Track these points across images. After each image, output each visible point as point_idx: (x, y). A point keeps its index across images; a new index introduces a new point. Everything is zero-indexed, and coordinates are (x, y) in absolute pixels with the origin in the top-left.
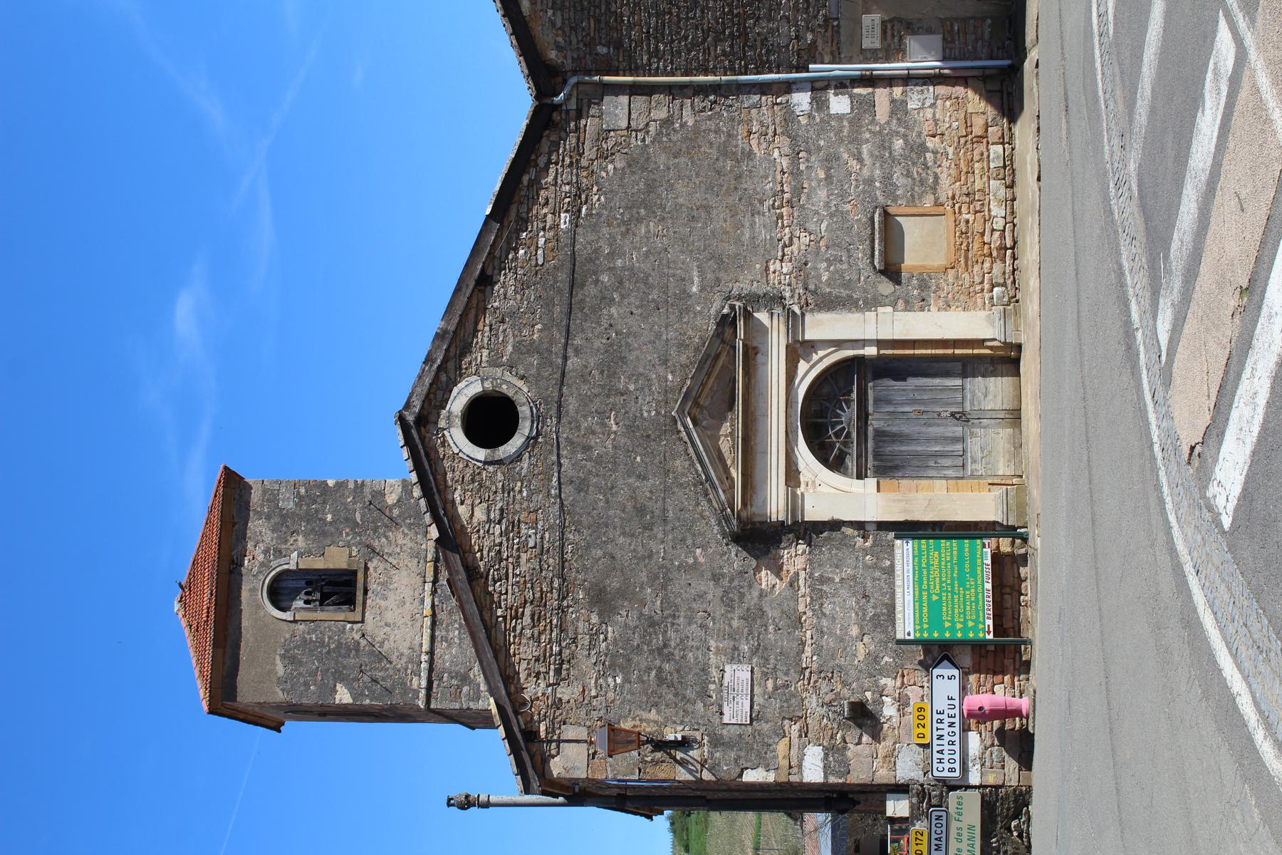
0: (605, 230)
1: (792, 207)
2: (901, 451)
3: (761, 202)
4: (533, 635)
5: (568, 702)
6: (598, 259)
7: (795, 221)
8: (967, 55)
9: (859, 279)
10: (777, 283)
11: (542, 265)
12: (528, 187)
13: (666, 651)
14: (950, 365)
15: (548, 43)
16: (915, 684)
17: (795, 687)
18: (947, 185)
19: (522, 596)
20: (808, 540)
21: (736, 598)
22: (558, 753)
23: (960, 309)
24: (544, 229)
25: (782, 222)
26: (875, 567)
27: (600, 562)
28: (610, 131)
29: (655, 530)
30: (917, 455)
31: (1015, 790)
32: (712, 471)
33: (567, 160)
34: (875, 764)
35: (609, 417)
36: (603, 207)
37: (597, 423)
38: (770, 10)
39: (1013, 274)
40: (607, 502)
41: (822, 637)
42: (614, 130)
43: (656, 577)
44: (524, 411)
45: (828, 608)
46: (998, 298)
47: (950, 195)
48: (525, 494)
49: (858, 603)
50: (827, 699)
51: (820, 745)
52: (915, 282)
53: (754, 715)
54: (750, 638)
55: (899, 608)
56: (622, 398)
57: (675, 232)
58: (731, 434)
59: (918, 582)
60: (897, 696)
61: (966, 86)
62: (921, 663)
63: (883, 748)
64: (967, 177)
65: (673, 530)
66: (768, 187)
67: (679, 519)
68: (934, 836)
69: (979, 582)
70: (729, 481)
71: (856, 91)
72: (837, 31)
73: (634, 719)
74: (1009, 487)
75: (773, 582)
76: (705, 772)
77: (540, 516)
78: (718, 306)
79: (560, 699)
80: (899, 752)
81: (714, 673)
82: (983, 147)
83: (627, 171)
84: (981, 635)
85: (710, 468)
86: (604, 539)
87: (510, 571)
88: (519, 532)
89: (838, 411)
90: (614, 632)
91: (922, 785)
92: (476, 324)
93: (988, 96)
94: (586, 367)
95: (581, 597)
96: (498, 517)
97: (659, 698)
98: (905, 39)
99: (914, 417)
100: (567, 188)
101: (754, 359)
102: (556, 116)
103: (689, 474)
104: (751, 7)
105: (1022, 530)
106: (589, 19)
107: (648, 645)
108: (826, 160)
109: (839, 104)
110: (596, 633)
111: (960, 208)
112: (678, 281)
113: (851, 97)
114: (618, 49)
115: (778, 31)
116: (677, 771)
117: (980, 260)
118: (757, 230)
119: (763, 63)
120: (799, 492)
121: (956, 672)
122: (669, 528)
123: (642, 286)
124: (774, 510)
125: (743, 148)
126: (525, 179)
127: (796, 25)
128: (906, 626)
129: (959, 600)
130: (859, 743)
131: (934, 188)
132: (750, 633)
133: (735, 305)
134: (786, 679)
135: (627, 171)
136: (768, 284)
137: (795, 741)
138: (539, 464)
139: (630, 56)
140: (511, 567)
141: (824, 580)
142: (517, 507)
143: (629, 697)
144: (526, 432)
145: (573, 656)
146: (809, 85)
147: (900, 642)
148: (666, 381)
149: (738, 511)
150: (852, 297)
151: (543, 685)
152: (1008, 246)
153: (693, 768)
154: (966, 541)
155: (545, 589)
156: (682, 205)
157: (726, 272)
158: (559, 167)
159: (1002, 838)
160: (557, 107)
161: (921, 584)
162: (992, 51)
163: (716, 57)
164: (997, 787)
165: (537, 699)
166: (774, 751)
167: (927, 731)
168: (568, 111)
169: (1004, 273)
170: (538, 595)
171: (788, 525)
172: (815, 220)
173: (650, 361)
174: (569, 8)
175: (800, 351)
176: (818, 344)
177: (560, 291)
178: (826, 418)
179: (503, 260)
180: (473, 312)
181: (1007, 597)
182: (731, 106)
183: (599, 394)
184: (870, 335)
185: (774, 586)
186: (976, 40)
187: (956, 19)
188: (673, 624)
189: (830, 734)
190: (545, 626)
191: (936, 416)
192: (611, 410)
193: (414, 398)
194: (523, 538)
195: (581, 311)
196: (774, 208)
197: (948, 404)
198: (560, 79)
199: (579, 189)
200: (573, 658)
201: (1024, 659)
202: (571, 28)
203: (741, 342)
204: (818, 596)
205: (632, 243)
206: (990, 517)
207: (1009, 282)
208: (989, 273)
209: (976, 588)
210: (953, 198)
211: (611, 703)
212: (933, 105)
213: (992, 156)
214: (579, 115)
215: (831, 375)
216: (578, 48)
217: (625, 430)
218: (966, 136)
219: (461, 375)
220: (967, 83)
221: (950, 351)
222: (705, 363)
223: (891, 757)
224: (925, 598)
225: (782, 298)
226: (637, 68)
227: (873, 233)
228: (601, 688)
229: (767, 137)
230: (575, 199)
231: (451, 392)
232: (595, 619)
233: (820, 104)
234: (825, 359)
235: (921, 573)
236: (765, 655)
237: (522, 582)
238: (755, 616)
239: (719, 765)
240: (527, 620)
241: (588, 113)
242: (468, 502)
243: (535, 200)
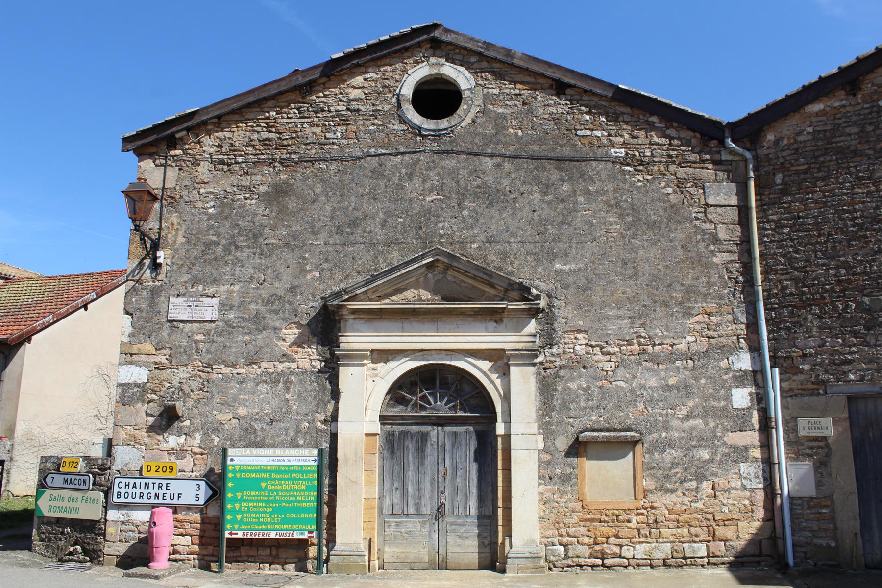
0: (611, 187)
1: (639, 354)
2: (408, 457)
3: (643, 325)
4: (252, 140)
5: (197, 171)
6: (584, 181)
7: (626, 357)
8: (797, 521)
9: (570, 418)
10: (566, 340)
11: (576, 135)
12: (647, 121)
13: (233, 248)
14: (489, 503)
15: (781, 132)
16: (194, 464)
17: (196, 359)
18: (665, 502)
19: (285, 131)
20: (324, 370)
21: (275, 307)
22: (157, 165)
23: (543, 514)
24: (610, 135)
25: (624, 345)
26: (298, 431)
27: (310, 191)
28: (703, 189)
29: (337, 236)
30: (404, 471)
31: (101, 551)
32: (382, 281)
33: (674, 153)
34: (129, 427)
35: (438, 194)
36: (632, 185)
37: (433, 185)
38: (830, 328)
39: (577, 566)
40: (362, 195)
41: (238, 383)
42: (704, 192)
43: (295, 238)
44: (444, 123)
45: (263, 387)
46: (553, 551)
47: (655, 505)
48: (371, 128)
49: (266, 414)
50: (185, 387)
51: (148, 380)
52: (568, 470)
53: (175, 323)
54: (240, 319)
55: (255, 451)
56: (456, 205)
57: (611, 247)
58: (421, 300)
59: (279, 470)
60: (185, 448)
61: (765, 520)
62: (212, 470)
63: (142, 435)
64: (673, 521)
66: (658, 331)
67: (346, 256)
68: (73, 477)
69: (277, 526)
70: (377, 299)
71: (755, 414)
72: (813, 393)
73: (179, 224)
74: (366, 558)
75: (287, 340)
76: (134, 283)
77: (352, 141)
78: (539, 286)
79: (199, 165)
80: (138, 449)
81: (212, 290)
82: (703, 536)
83: (667, 205)
84: (228, 526)
85: (386, 280)
86: (330, 193)
87: (306, 120)
88: (339, 125)
89: (446, 399)
90: (251, 205)
91: (110, 468)
92: (522, 83)
93: (755, 542)
94: (484, 173)
95: (282, 177)
96: (352, 108)
97: (194, 244)
98: (810, 460)
99: (440, 469)
100: (649, 154)
101: (491, 320)
102: (714, 143)
104: (832, 310)
105: (325, 569)
106: (807, 164)
107: (238, 233)
108: (686, 386)
109: (741, 397)
110: (251, 191)
111: (642, 514)
112: (565, 251)
113: (749, 408)
114: (780, 193)
115: (810, 337)
116: (134, 261)
117: (590, 533)
118: (616, 322)
119: (777, 324)
120: (365, 361)
121: (202, 502)
122: (338, 248)
123: (559, 220)
125: (694, 308)
126: (654, 119)
127: (816, 354)
128: (239, 458)
129: (260, 507)
130: (147, 414)
131: (661, 489)
132: (244, 320)
133: (540, 300)
134: (204, 351)
135: (667, 205)
136: (564, 332)
137: (152, 359)
138: (397, 138)
139: (775, 204)
140: (309, 120)
141: (288, 384)
142: (361, 122)
143: (197, 219)
144: (425, 126)
145: (233, 173)
146: (758, 368)
147: (224, 452)
148: (471, 242)
149: (345, 306)
150: (553, 411)
151: (212, 150)
152: (605, 561)
153: (136, 273)
154: (315, 516)
155: (290, 148)
156: (637, 254)
157: (575, 294)
158: (667, 146)
159: (70, 537)
160: (722, 143)
161: (278, 472)
162: (801, 546)
163: (780, 281)
164: (104, 535)
165: (201, 147)
166: (145, 341)
167: (152, 474)
168: (719, 152)
169: (578, 557)
170: (285, 142)
171: (334, 351)
172: (627, 375)
173: (490, 228)
174: (815, 145)
175: (500, 363)
176: (507, 379)
177: (554, 150)
178: (440, 388)
179: (580, 102)
180: (532, 80)
181: (268, 551)
182: (734, 296)
183: (459, 186)
184: (515, 428)
185: (284, 340)
186: (812, 531)
187: (833, 511)
188: (255, 254)
189: (156, 389)
190: (259, 150)
191: (441, 489)
192: (445, 196)
193: (453, 36)
194: (334, 129)
195: (535, 168)
196: (637, 337)
197: (452, 501)
198: (748, 145)
199: (648, 164)
200: (232, 173)
201: (212, 564)
202: (797, 150)
203: (504, 306)
204: (273, 379)
205: (600, 210)
206: (338, 539)
207: (569, 561)
208: (578, 542)
209: (271, 523)
210: (652, 508)
211: (194, 205)
212: (744, 488)
213: (695, 545)
214: (715, 163)
216: (778, 158)
217: (426, 208)
218: (714, 520)
219: (476, 73)
220: (768, 520)
221: (500, 504)
222: (484, 273)
223: (133, 442)
224: (264, 475)
225: (551, 345)
226: (765, 211)
227: (615, 430)
228: (206, 197)
229: (706, 330)
230: (638, 160)
231: (461, 65)
232: (263, 189)
233: (740, 379)
234: (493, 385)
235: (286, 472)
236: (225, 333)
237: (296, 129)
238: (258, 323)
239: (137, 294)
240: (265, 135)
241: (719, 170)
242: (366, 84)
243: (636, 126)
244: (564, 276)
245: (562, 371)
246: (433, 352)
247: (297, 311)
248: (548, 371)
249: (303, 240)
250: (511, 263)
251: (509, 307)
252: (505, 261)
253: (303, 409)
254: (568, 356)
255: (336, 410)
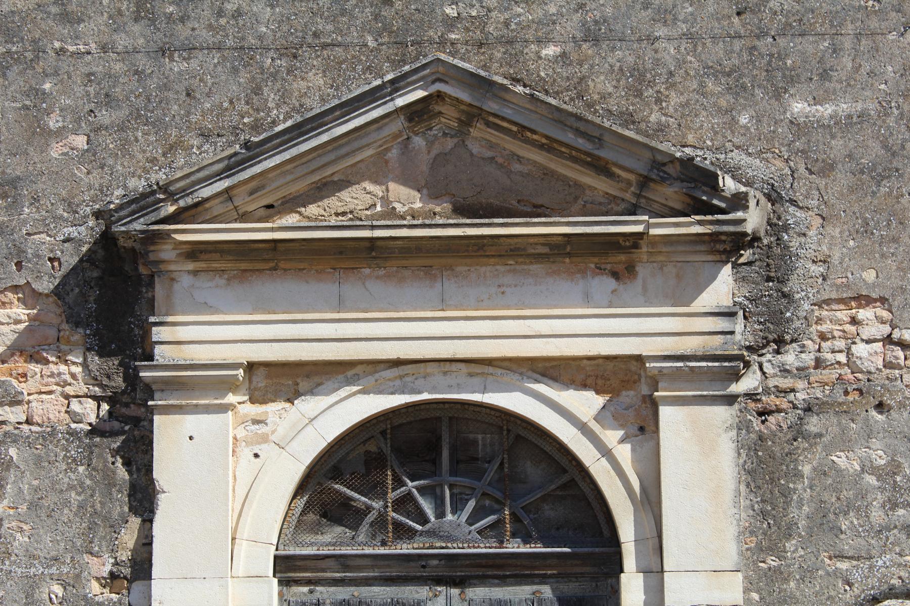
9: (841, 557)
10: (823, 328)
29: (136, 28)
58: (391, 213)
65: (137, 72)
67: (166, 87)
70: (263, 212)
85: (287, 155)
89: (471, 504)
103: (285, 109)
120: (231, 398)
122: (142, 62)
124: (183, 333)
133: (745, 208)
136: (819, 305)
148: (539, 41)
149: (168, 234)
150: (789, 537)
157: (852, 190)
171: (136, 370)
175: (628, 396)
176: (652, 443)
178: (453, 472)
203: (639, 228)
215: (572, 483)
222: (579, 132)
225: (780, 342)
244: (818, 136)
245: (814, 419)
246: (431, 368)
247: (21, 251)
248: (771, 419)
249: (34, 41)
250: (658, 101)
251: (654, 231)
252: (639, 94)
253: (47, 545)
254: (830, 375)
255: (146, 543)
